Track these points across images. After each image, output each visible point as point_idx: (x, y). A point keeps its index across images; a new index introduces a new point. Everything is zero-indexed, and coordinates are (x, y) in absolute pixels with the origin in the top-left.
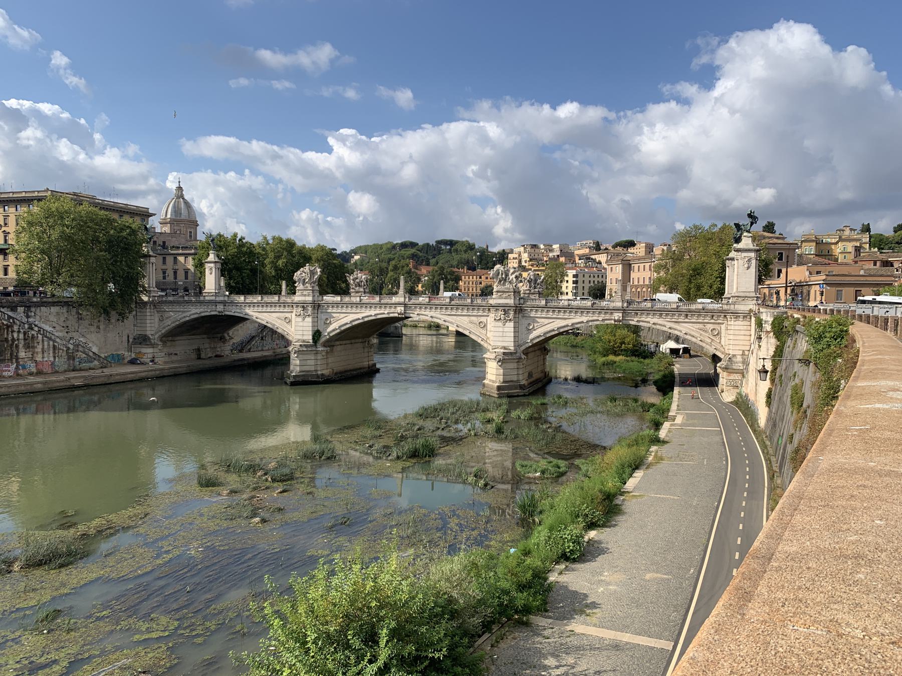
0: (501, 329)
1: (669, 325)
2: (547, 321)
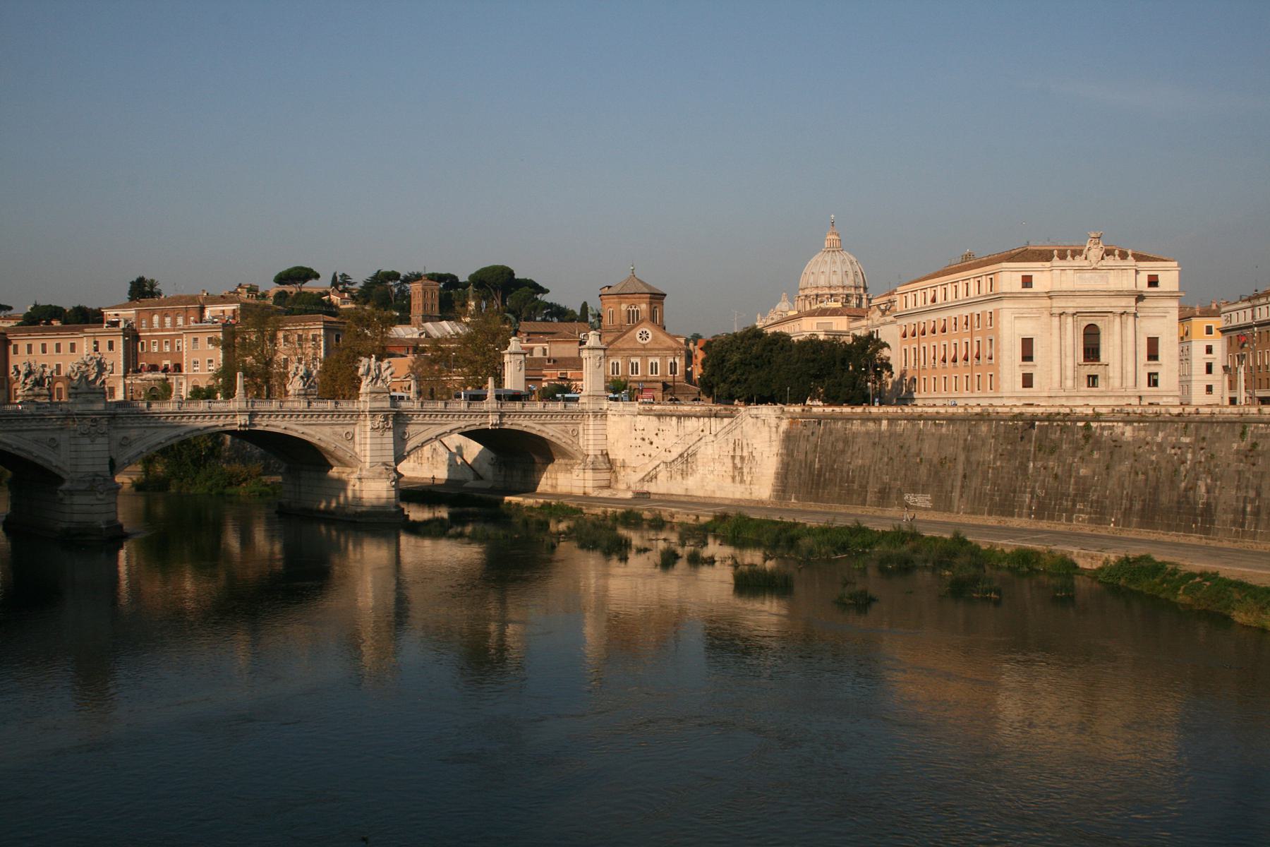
0: (379, 441)
1: (538, 427)
2: (422, 428)
